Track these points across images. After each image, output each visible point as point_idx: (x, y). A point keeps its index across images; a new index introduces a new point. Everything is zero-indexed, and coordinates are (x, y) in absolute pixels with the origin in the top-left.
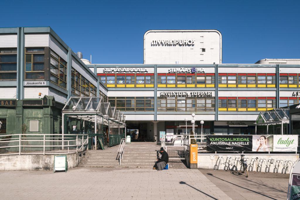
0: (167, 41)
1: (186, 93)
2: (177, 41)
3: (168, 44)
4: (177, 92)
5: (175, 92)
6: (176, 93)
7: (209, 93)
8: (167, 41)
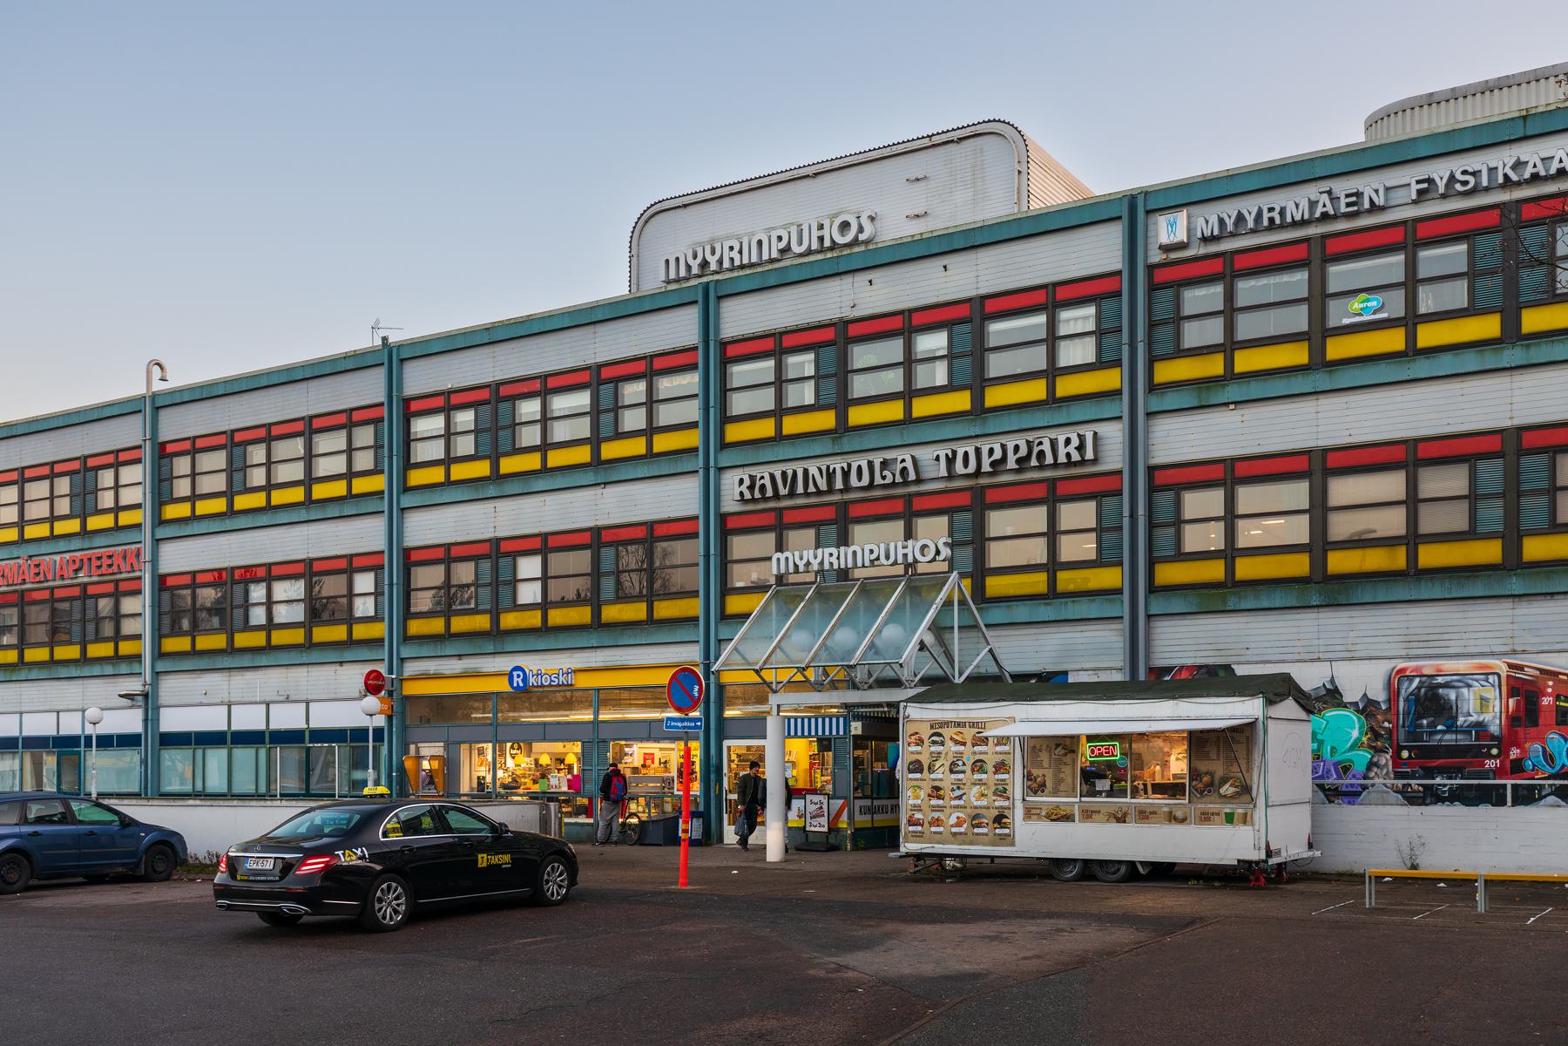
0: (731, 248)
1: (900, 466)
2: (780, 238)
3: (737, 263)
4: (838, 464)
5: (823, 463)
6: (830, 476)
7: (1068, 441)
8: (731, 248)
